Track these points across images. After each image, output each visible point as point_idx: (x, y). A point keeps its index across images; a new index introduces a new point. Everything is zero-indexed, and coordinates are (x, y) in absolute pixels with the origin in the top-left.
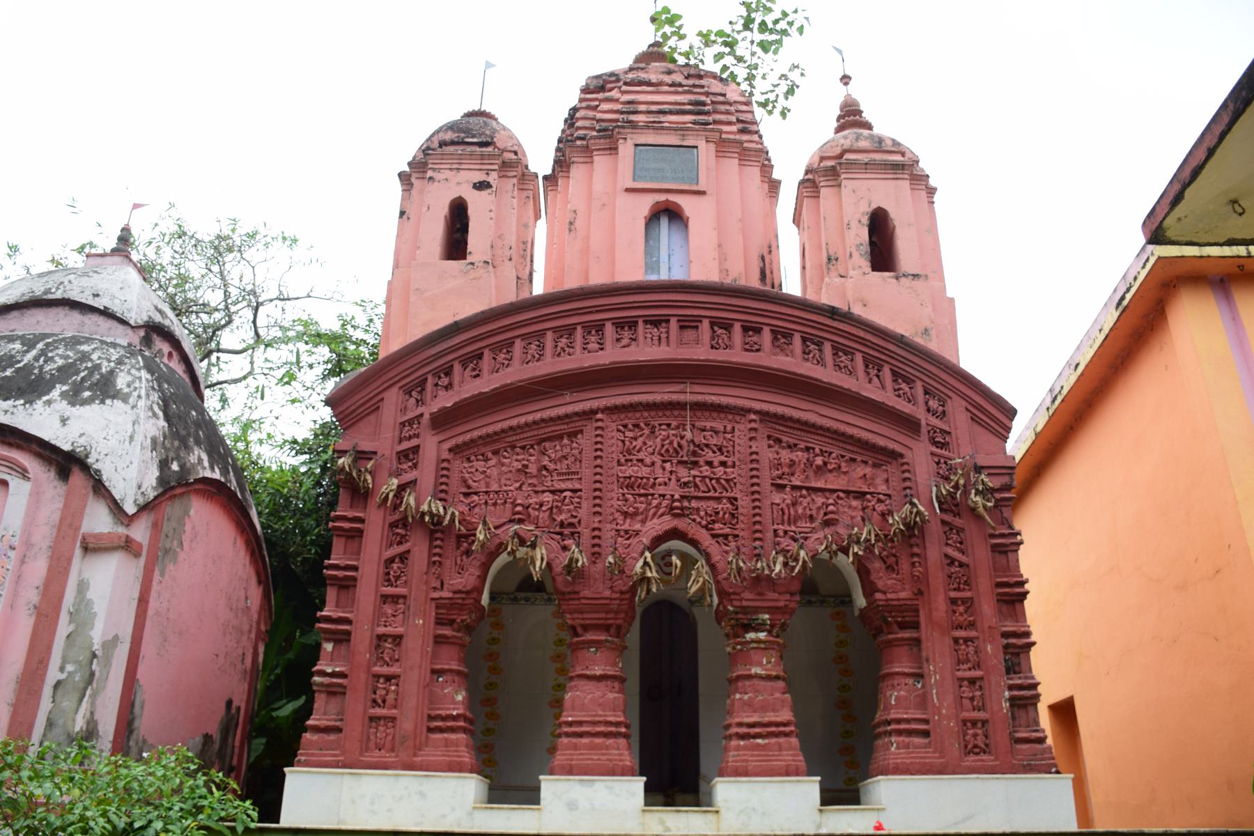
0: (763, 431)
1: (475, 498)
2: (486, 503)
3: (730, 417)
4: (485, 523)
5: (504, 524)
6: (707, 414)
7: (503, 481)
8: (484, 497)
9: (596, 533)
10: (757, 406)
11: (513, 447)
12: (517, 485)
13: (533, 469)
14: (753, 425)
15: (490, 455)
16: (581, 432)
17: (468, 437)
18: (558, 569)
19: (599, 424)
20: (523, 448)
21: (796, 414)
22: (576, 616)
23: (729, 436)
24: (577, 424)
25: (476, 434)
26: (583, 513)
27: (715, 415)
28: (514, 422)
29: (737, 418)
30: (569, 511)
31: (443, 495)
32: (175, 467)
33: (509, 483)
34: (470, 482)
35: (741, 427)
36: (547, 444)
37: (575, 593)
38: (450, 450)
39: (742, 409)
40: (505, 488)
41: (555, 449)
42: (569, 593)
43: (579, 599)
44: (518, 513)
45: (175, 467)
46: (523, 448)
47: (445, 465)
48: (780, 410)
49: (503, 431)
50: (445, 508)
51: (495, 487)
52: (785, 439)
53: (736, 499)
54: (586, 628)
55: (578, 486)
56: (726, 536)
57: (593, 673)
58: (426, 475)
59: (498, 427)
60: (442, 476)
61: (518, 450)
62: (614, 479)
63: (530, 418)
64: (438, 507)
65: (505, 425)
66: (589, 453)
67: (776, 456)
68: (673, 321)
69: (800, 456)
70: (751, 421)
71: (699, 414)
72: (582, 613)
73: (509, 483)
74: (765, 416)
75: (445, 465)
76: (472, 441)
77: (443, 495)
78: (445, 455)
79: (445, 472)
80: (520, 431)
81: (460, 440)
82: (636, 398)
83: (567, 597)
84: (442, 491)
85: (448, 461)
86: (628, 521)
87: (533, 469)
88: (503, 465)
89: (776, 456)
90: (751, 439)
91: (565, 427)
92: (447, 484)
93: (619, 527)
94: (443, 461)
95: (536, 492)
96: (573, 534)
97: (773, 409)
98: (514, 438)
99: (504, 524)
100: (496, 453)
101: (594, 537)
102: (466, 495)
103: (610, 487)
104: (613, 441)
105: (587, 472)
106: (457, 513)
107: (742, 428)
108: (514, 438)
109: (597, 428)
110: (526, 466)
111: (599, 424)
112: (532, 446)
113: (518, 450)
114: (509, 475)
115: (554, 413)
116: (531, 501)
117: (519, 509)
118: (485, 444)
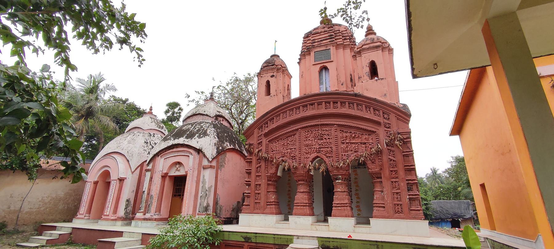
0: (339, 129)
1: (274, 152)
2: (276, 153)
3: (330, 126)
4: (275, 158)
5: (280, 158)
6: (324, 126)
7: (280, 148)
8: (276, 152)
9: (300, 158)
10: (337, 123)
11: (281, 139)
12: (283, 148)
13: (286, 144)
14: (336, 128)
15: (277, 142)
16: (296, 134)
17: (271, 138)
18: (291, 167)
19: (299, 132)
20: (283, 139)
21: (346, 124)
22: (296, 178)
23: (330, 131)
24: (295, 132)
25: (273, 137)
26: (297, 154)
27: (326, 126)
28: (281, 134)
29: (332, 126)
30: (294, 153)
31: (267, 152)
32: (221, 148)
33: (281, 148)
34: (273, 148)
35: (332, 129)
36: (289, 138)
37: (296, 173)
38: (268, 142)
39: (333, 124)
40: (280, 149)
41: (290, 139)
42: (294, 173)
43: (296, 174)
44: (283, 155)
45: (221, 148)
46: (283, 139)
47: (267, 145)
48: (343, 123)
49: (279, 136)
50: (267, 155)
51: (278, 149)
52: (344, 130)
53: (332, 147)
54: (299, 180)
55: (296, 147)
56: (330, 157)
57: (301, 191)
58: (263, 148)
59: (277, 135)
60: (267, 148)
61: (282, 140)
62: (303, 145)
63: (284, 132)
64: (266, 155)
65: (279, 134)
66: (298, 139)
67: (342, 135)
68: (316, 103)
69: (348, 134)
70: (335, 127)
71: (322, 126)
72: (298, 177)
73: (281, 148)
74: (339, 125)
75: (267, 145)
76: (272, 139)
77: (267, 152)
78: (267, 143)
79: (267, 147)
80: (282, 135)
81: (270, 139)
82: (307, 125)
83: (294, 174)
84: (267, 151)
85: (268, 144)
86: (307, 154)
87: (286, 144)
88: (279, 144)
89: (342, 135)
90: (335, 132)
91: (292, 133)
92: (268, 150)
93: (305, 156)
94: (267, 144)
95: (287, 149)
96: (295, 159)
97: (340, 123)
98: (282, 137)
99: (280, 158)
100: (278, 141)
101: (299, 159)
102: (272, 151)
103: (303, 147)
104: (303, 135)
105: (297, 144)
106: (270, 156)
107: (333, 129)
108: (282, 137)
109: (299, 133)
110: (284, 144)
111: (299, 132)
112: (285, 139)
113: (282, 140)
114: (281, 146)
115: (289, 130)
116: (285, 152)
117: (283, 154)
118: (275, 139)
